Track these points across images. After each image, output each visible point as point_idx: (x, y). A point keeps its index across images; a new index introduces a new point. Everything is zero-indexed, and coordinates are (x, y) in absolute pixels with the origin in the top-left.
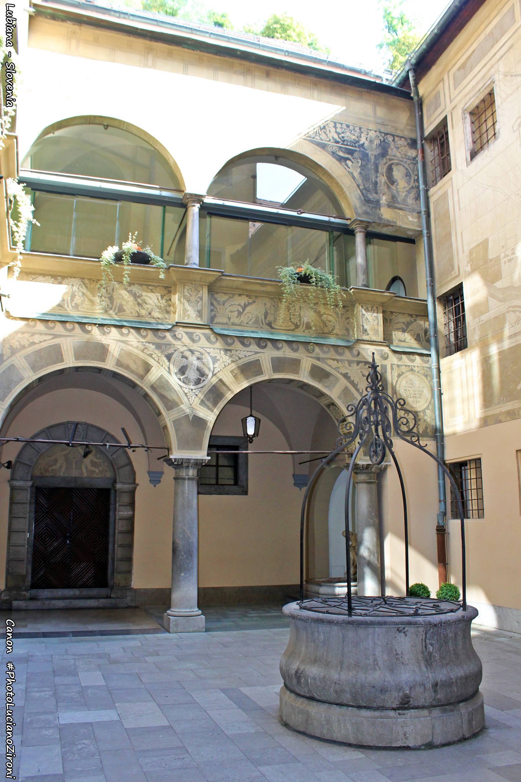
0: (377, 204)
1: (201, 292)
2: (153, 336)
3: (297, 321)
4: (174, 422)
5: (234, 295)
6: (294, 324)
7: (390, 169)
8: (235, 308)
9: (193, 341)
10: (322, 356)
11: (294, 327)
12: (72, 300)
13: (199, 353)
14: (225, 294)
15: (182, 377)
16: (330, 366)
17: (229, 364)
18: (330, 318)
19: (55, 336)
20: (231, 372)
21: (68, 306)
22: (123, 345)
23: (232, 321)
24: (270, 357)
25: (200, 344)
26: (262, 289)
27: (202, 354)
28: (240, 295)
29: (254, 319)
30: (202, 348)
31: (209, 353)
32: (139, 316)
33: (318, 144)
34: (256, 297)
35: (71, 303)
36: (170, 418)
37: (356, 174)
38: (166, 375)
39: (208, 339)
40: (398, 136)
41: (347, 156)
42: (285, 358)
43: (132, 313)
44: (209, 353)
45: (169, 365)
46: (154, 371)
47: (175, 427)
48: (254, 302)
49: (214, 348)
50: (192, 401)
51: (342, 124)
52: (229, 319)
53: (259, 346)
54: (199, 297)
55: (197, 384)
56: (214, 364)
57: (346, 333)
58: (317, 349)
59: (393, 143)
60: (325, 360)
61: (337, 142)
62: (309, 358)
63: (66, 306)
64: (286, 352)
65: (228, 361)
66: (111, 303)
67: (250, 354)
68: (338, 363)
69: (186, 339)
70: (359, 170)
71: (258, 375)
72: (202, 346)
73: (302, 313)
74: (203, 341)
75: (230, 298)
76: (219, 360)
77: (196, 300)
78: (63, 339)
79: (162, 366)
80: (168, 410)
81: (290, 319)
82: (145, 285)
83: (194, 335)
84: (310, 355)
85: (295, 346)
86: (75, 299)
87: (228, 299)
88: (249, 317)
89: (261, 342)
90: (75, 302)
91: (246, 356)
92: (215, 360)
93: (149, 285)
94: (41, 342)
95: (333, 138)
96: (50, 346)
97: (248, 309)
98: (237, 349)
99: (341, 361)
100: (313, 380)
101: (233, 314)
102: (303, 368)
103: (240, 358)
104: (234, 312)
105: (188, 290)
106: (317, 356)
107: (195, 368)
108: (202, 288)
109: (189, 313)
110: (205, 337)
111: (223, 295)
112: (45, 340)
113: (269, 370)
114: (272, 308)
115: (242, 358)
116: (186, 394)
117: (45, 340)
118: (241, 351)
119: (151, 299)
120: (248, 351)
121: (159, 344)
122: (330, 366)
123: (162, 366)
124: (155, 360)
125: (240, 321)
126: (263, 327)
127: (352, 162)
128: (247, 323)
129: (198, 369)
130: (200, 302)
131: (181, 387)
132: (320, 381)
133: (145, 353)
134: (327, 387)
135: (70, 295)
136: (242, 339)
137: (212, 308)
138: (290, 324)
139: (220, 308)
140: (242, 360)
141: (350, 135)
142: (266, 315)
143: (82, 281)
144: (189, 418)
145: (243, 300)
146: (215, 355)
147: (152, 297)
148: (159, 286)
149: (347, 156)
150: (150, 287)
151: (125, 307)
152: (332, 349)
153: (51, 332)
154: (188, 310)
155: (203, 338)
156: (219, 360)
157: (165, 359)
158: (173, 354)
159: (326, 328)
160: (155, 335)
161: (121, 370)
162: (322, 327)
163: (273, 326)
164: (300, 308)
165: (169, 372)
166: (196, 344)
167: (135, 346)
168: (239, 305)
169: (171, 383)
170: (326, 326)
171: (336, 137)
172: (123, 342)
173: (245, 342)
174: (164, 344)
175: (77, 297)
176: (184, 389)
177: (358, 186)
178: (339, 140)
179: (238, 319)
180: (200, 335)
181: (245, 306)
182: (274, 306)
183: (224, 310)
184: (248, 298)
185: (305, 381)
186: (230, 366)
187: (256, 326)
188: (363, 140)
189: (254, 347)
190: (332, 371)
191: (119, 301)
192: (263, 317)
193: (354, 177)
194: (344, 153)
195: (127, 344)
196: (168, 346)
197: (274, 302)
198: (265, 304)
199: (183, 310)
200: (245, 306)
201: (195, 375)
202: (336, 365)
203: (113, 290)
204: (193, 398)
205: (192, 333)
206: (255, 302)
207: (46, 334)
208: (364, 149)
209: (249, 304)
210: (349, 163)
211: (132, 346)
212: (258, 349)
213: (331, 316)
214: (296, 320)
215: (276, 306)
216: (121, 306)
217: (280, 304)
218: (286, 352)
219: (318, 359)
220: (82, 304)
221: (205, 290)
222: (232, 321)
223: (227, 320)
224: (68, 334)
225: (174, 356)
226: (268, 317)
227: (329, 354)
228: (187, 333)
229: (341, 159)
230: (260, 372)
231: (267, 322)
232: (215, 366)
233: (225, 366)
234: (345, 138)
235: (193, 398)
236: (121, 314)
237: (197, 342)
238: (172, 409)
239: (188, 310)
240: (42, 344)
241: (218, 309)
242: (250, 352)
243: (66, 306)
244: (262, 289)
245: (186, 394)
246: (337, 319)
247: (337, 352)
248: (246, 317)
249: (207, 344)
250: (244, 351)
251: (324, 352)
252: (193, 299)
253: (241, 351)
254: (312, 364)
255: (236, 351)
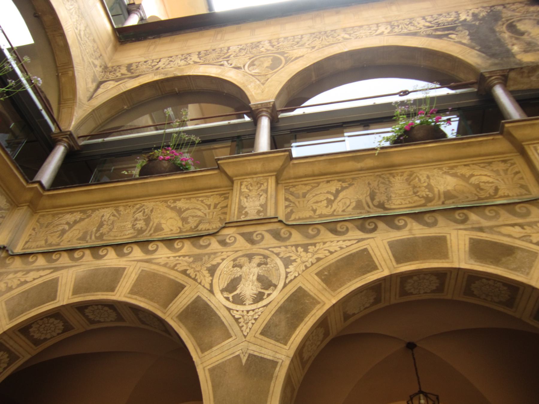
0: (508, 54)
1: (265, 184)
2: (191, 246)
3: (428, 193)
4: (212, 371)
5: (318, 184)
6: (423, 197)
7: (512, 27)
8: (322, 197)
9: (252, 242)
10: (485, 223)
11: (423, 202)
12: (98, 230)
13: (261, 257)
14: (305, 185)
15: (230, 296)
16: (509, 236)
17: (312, 264)
18: (484, 179)
19: (56, 269)
20: (317, 274)
21: (91, 238)
22: (145, 265)
23: (318, 213)
24: (385, 242)
25: (263, 244)
26: (359, 165)
27: (266, 257)
28: (328, 182)
29: (354, 204)
30: (267, 249)
31: (278, 254)
32: (181, 232)
33: (407, 34)
34: (353, 179)
35: (96, 233)
36: (205, 365)
37: (465, 41)
38: (205, 296)
39: (276, 235)
40: (508, 4)
41: (446, 32)
42: (415, 238)
43: (172, 230)
44: (278, 254)
45: (212, 280)
46: (187, 293)
47: (213, 381)
48: (351, 185)
49: (286, 247)
50: (248, 330)
51: (432, 16)
52: (314, 211)
53: (362, 229)
54: (262, 190)
55: (258, 302)
56: (286, 267)
57: (524, 191)
58: (473, 217)
59: (505, 9)
60: (495, 229)
61: (429, 27)
62: (460, 232)
63: (88, 238)
64: (416, 230)
65: (310, 260)
66: (146, 225)
67: (349, 243)
68: (523, 228)
69: (241, 242)
70: (468, 37)
71: (369, 272)
72: (266, 246)
73: (433, 182)
74: (269, 241)
75: (313, 187)
76: (295, 261)
77: (259, 194)
78: (64, 272)
79: (200, 283)
80: (203, 350)
81: (415, 193)
82: (193, 198)
83: (255, 235)
84: (462, 227)
85: (428, 218)
86: (102, 229)
87: (311, 189)
88: (345, 203)
89: (366, 224)
90: (101, 232)
91: (341, 248)
92: (287, 262)
93: (200, 197)
94: (34, 279)
95: (424, 26)
96: (44, 282)
97: (341, 195)
98: (325, 241)
99: (530, 224)
100: (481, 262)
101: (319, 204)
102: (455, 248)
103: (331, 253)
104: (321, 201)
105: (247, 186)
106: (477, 226)
107: (255, 278)
108: (267, 180)
109: (246, 210)
110: (272, 235)
111: (304, 187)
112: (41, 277)
113: (388, 262)
114: (381, 185)
115: (336, 251)
116: (237, 320)
117: (41, 277)
118: (332, 242)
119: (200, 210)
120: (344, 241)
121: (199, 255)
122: (509, 236)
123: (200, 283)
124: (190, 277)
125: (332, 210)
126: (371, 210)
127: (457, 35)
128: (343, 211)
129: (260, 279)
130: (264, 195)
131: (229, 310)
132: (496, 261)
133: (177, 270)
134: (515, 270)
135: (97, 225)
136: (332, 226)
137: (287, 203)
138: (416, 198)
139: (299, 202)
140: (335, 255)
141: (444, 19)
142: (372, 197)
143: (115, 210)
144: (241, 361)
145: (334, 187)
146: (288, 255)
147: (202, 208)
148: (212, 195)
149: (446, 32)
150: (200, 199)
151: (164, 226)
152: (503, 212)
153: (53, 265)
154: (246, 208)
155: (267, 236)
156: (295, 261)
157: (206, 273)
158: (219, 264)
159: (481, 192)
160: (194, 245)
161: (136, 299)
162: (475, 192)
163: (386, 206)
164: (428, 177)
165: (211, 291)
166: (257, 246)
167: (163, 263)
168: (328, 192)
169: (212, 306)
170: (482, 189)
171: (428, 24)
172: (147, 261)
173: (339, 229)
174: (207, 254)
175: (105, 226)
176: (234, 313)
177: (473, 48)
178: (433, 25)
179: (329, 209)
180: (264, 233)
181: (338, 192)
182: (383, 183)
183: (306, 202)
184: (340, 183)
185: (463, 266)
186: (314, 267)
187: (359, 211)
188: (463, 17)
189: (355, 234)
190: (518, 243)
191: (156, 221)
192: (368, 199)
193: (464, 44)
194: (442, 31)
195: (152, 263)
196: (212, 256)
197: (383, 178)
198: (369, 184)
199: (239, 208)
200: (338, 192)
201: (254, 288)
202: (520, 232)
203: (152, 211)
204: (250, 325)
205: (251, 233)
206: (353, 184)
207: (44, 269)
208: (468, 22)
209: (343, 189)
210: (453, 36)
211: (158, 264)
212: (360, 234)
213: (486, 175)
214: (424, 192)
215: (387, 183)
216: (159, 224)
217: (392, 180)
218: (416, 230)
219: (481, 229)
220: (109, 232)
221: (272, 181)
222: (318, 213)
223: (311, 214)
224: (74, 264)
225: (221, 266)
226: (376, 197)
227: (501, 219)
228: (242, 235)
229: (439, 37)
230: (372, 267)
231: (376, 202)
232: (288, 270)
233: (307, 268)
234: (440, 22)
235: (250, 325)
236: (157, 234)
237: (259, 243)
238: (211, 347)
239: (246, 208)
240: (36, 281)
241: (297, 204)
242: (349, 240)
243: (88, 238)
244: (359, 165)
245: (237, 320)
246: (498, 177)
247: (514, 214)
248: (341, 204)
249: (275, 243)
250: (338, 241)
251: (490, 218)
252: (254, 193)
253: (332, 242)
254: (470, 239)
255: (324, 243)
